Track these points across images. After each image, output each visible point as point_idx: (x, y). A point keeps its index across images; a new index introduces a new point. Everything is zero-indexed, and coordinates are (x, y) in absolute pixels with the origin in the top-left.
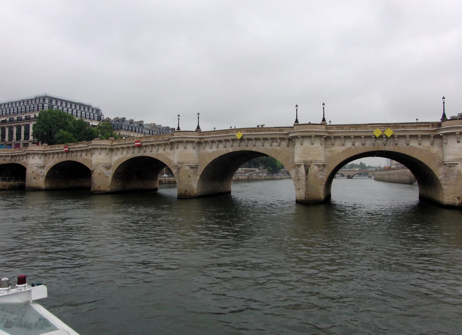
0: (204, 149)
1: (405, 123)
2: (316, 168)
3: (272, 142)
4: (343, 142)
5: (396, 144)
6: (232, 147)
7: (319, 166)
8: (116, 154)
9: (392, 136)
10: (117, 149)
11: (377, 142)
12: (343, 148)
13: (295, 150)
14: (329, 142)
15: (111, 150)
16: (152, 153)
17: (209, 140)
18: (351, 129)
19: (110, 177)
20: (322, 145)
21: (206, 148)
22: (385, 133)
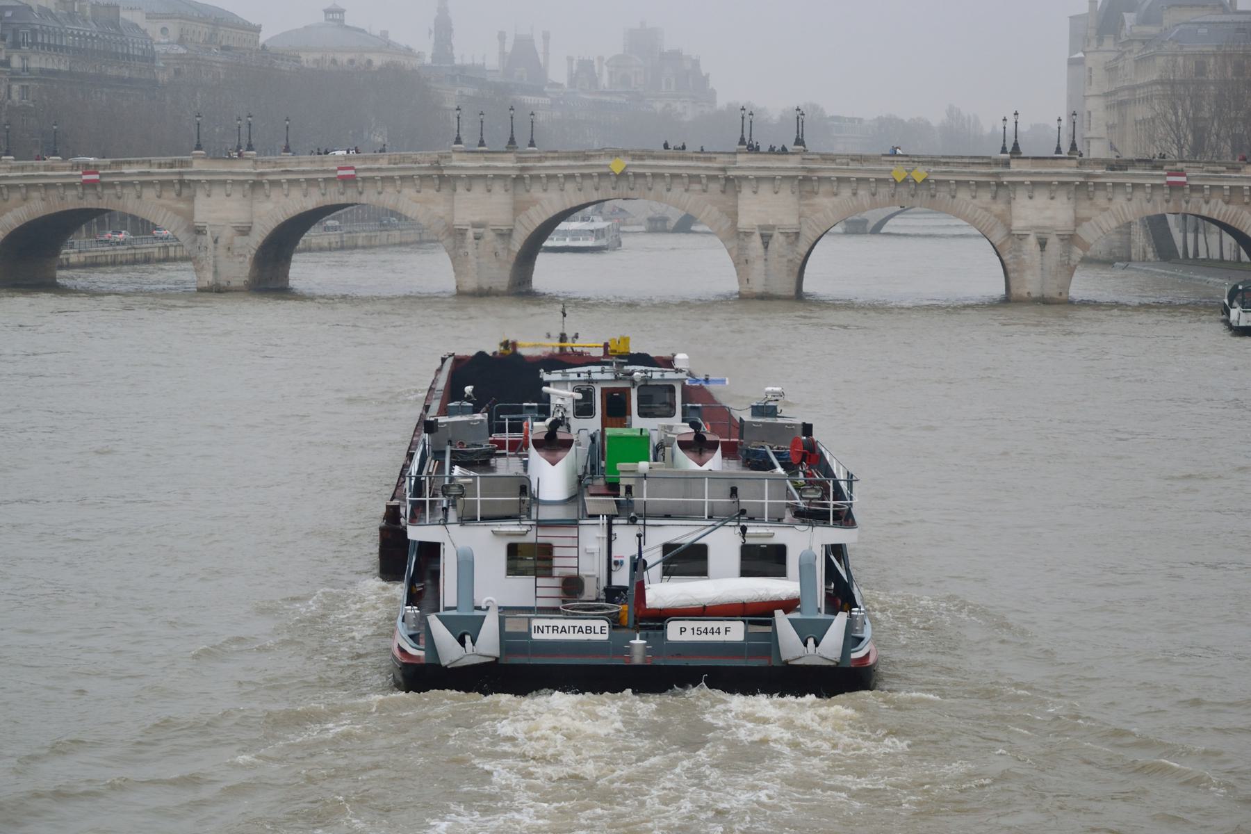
0: (528, 191)
1: (949, 157)
2: (782, 238)
3: (690, 182)
4: (835, 188)
5: (933, 196)
6: (597, 189)
7: (787, 235)
8: (268, 196)
9: (926, 181)
10: (275, 184)
11: (899, 189)
12: (835, 199)
13: (740, 202)
14: (808, 188)
15: (256, 185)
16: (382, 197)
17: (543, 173)
18: (851, 163)
19: (249, 256)
20: (793, 193)
21: (532, 191)
22: (912, 174)
